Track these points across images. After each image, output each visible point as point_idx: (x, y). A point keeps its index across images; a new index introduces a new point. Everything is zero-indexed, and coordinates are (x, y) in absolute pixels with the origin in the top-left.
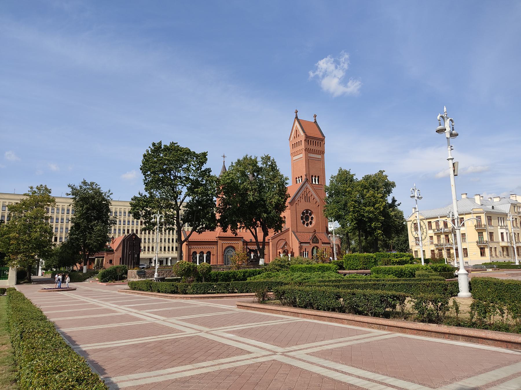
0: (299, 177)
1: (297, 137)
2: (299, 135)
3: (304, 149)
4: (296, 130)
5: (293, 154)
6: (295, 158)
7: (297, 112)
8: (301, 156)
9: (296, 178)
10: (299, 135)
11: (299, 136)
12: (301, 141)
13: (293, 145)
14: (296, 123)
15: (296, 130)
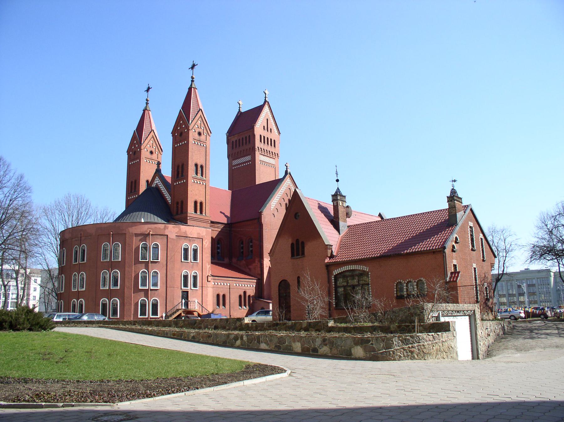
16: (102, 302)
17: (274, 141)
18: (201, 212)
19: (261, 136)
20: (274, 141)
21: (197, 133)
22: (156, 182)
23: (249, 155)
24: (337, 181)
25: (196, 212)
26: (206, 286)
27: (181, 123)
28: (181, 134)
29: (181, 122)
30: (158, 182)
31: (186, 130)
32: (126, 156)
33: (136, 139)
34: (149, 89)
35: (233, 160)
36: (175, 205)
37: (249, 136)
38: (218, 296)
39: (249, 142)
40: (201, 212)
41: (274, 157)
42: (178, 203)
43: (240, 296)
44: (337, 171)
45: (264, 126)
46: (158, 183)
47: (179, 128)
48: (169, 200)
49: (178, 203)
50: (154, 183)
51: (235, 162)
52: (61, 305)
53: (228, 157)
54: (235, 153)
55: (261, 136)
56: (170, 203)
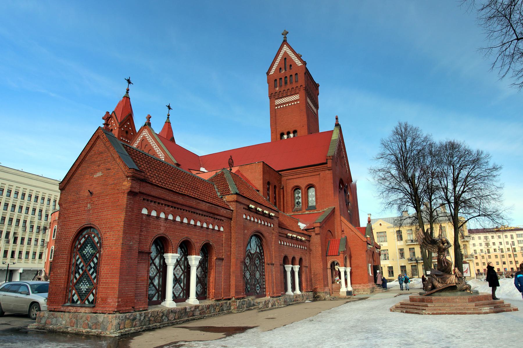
0: (288, 133)
1: (285, 70)
2: (291, 66)
3: (304, 86)
4: (285, 59)
5: (273, 96)
6: (278, 102)
7: (285, 33)
8: (296, 97)
9: (282, 134)
10: (291, 66)
11: (290, 69)
12: (296, 74)
13: (276, 80)
14: (284, 48)
15: (285, 59)
21: (125, 132)
29: (113, 121)
31: (115, 128)
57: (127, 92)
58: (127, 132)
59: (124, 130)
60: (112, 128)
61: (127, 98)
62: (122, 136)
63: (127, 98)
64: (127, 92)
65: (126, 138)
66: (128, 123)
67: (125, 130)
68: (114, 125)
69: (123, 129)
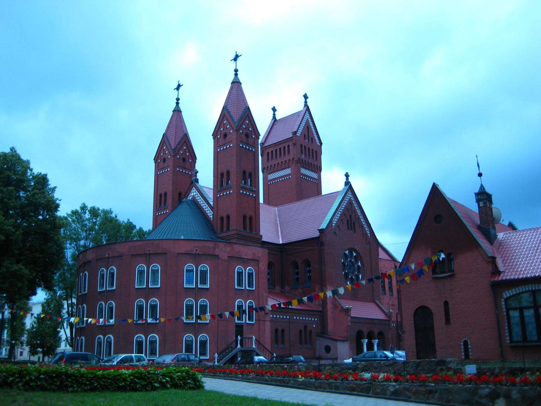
16: (136, 339)
17: (316, 152)
18: (251, 230)
19: (301, 145)
20: (316, 152)
21: (244, 135)
22: (192, 194)
23: (288, 167)
24: (480, 175)
25: (245, 228)
26: (263, 319)
27: (224, 123)
28: (225, 136)
29: (225, 122)
30: (195, 194)
31: (231, 131)
32: (153, 165)
33: (166, 144)
34: (179, 86)
35: (269, 174)
36: (219, 221)
37: (289, 146)
38: (276, 331)
39: (289, 152)
40: (251, 230)
41: (316, 171)
42: (222, 219)
43: (301, 332)
44: (478, 163)
45: (305, 135)
46: (196, 195)
47: (222, 129)
48: (211, 215)
49: (222, 219)
50: (190, 195)
51: (271, 177)
52: (82, 343)
53: (262, 171)
54: (271, 166)
55: (301, 145)
56: (212, 219)
57: (236, 75)
58: (247, 135)
59: (242, 133)
60: (225, 131)
61: (236, 84)
62: (242, 142)
63: (236, 84)
64: (236, 75)
65: (247, 144)
66: (247, 122)
67: (244, 132)
68: (228, 127)
69: (241, 132)
